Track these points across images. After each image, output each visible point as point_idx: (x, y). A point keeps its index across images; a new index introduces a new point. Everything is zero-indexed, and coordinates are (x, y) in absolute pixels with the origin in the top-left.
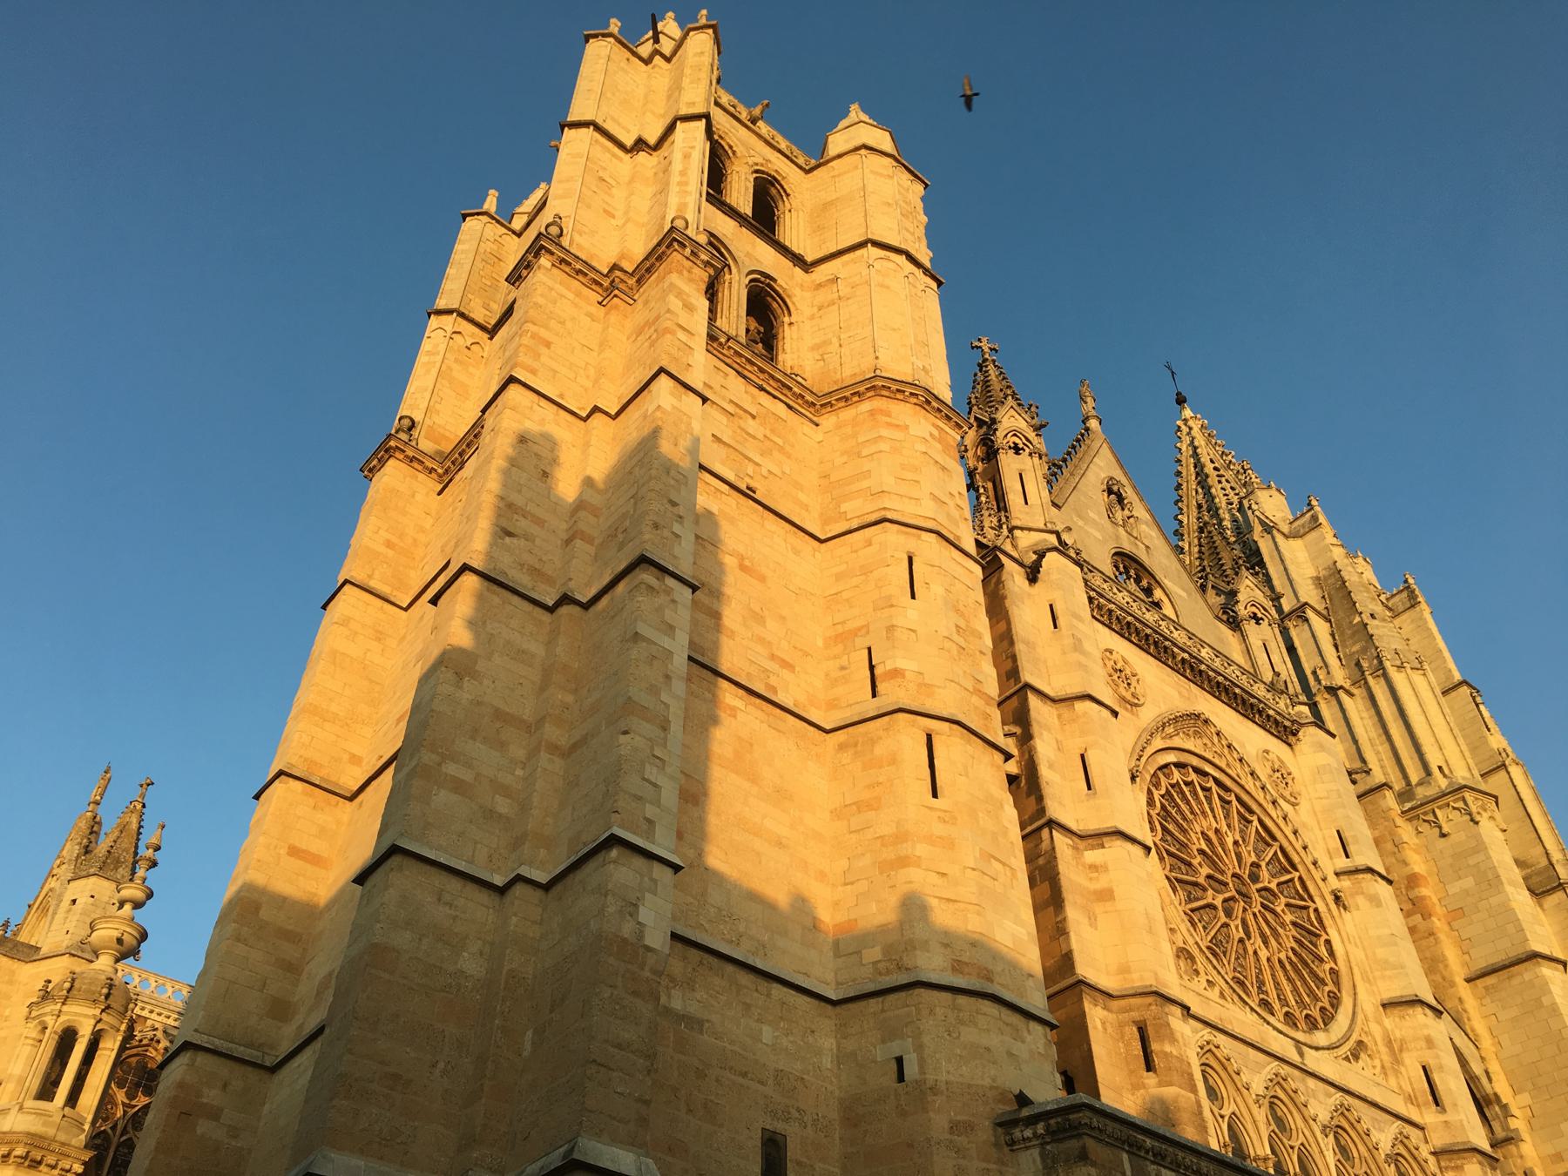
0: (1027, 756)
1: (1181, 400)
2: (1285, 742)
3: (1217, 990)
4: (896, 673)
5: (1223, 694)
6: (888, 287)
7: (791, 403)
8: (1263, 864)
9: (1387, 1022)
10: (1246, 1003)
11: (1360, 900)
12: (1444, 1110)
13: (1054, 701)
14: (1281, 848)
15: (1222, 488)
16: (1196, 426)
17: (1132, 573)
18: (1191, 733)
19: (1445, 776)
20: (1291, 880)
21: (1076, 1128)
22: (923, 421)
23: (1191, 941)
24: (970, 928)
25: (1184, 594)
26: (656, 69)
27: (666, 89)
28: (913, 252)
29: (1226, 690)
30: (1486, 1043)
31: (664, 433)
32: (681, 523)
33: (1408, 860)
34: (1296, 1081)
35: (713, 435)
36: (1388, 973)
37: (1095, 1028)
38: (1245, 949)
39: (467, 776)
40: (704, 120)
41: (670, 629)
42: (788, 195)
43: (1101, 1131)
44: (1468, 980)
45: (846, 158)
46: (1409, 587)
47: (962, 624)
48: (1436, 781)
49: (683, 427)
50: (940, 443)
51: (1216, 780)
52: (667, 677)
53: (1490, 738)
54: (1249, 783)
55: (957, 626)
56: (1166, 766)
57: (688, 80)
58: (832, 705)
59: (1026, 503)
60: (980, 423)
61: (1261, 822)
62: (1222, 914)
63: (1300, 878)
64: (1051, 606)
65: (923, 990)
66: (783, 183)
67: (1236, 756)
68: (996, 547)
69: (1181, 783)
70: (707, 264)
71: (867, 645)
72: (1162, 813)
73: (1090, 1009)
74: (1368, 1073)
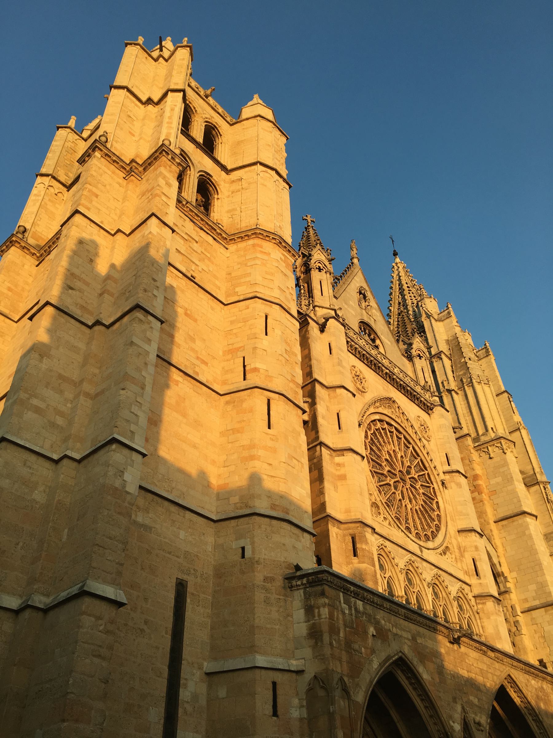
0: (313, 413)
1: (395, 254)
2: (427, 413)
3: (388, 522)
4: (256, 370)
5: (402, 389)
6: (266, 186)
7: (215, 237)
8: (413, 467)
10: (400, 528)
11: (453, 485)
12: (480, 578)
13: (327, 388)
14: (421, 460)
15: (410, 296)
16: (401, 266)
17: (367, 331)
18: (387, 406)
19: (494, 432)
20: (424, 474)
21: (321, 581)
22: (277, 252)
23: (378, 499)
24: (281, 489)
25: (389, 343)
26: (160, 64)
27: (164, 75)
28: (279, 170)
30: (500, 549)
31: (152, 245)
32: (158, 290)
33: (475, 468)
34: (418, 563)
35: (176, 249)
36: (461, 517)
37: (333, 536)
38: (401, 504)
39: (42, 405)
40: (182, 93)
41: (149, 341)
42: (221, 135)
43: (331, 582)
44: (495, 522)
45: (250, 121)
46: (486, 347)
47: (288, 349)
48: (490, 434)
49: (162, 243)
50: (284, 263)
52: (146, 364)
53: (514, 417)
54: (410, 430)
55: (286, 350)
57: (175, 72)
58: (224, 383)
59: (322, 295)
60: (304, 255)
61: (413, 448)
62: (393, 488)
63: (428, 474)
64: (329, 344)
65: (256, 517)
66: (219, 129)
67: (405, 418)
68: (306, 314)
69: (381, 429)
70: (179, 164)
71: (243, 355)
72: (371, 442)
73: (331, 528)
74: (449, 560)
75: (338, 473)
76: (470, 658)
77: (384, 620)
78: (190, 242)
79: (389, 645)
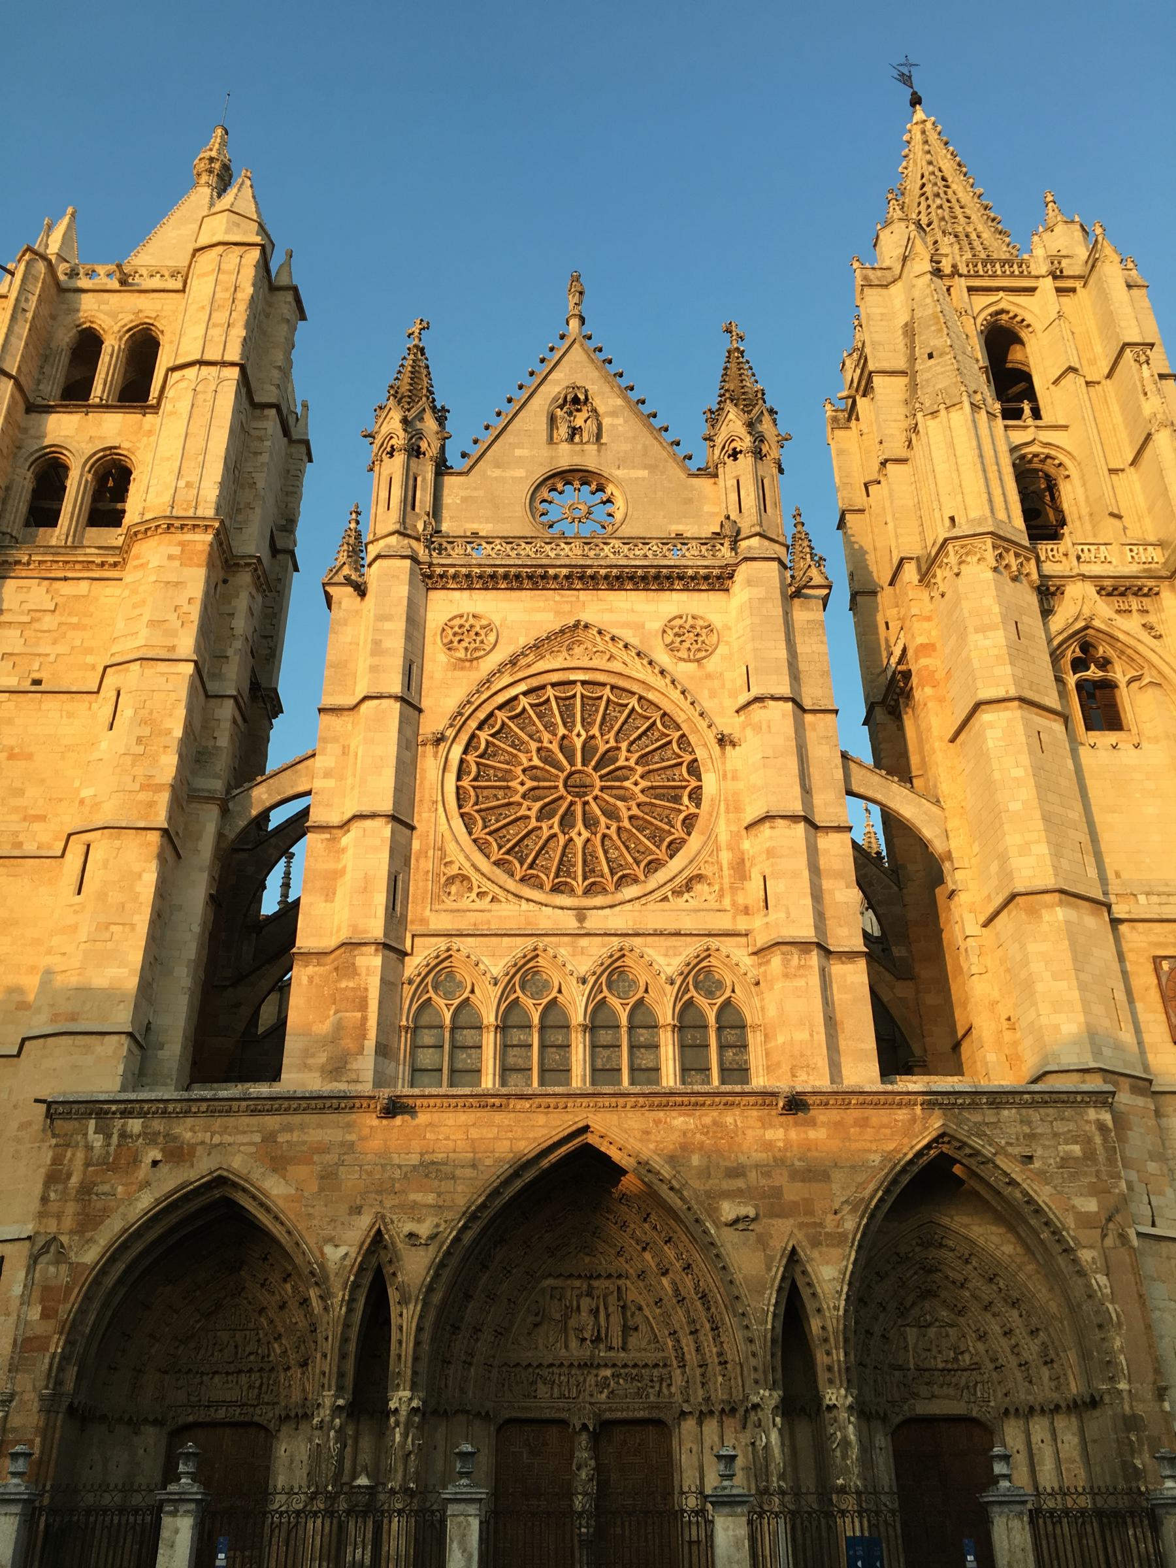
3: (490, 897)
10: (521, 897)
11: (749, 732)
14: (665, 714)
17: (577, 484)
20: (670, 742)
25: (644, 473)
29: (631, 578)
36: (754, 796)
37: (300, 984)
42: (162, 332)
44: (952, 740)
47: (146, 731)
50: (180, 559)
51: (584, 683)
56: (516, 698)
62: (533, 820)
63: (683, 735)
69: (528, 707)
75: (340, 866)
76: (442, 1129)
77: (191, 1130)
78: (38, 620)
79: (192, 1166)
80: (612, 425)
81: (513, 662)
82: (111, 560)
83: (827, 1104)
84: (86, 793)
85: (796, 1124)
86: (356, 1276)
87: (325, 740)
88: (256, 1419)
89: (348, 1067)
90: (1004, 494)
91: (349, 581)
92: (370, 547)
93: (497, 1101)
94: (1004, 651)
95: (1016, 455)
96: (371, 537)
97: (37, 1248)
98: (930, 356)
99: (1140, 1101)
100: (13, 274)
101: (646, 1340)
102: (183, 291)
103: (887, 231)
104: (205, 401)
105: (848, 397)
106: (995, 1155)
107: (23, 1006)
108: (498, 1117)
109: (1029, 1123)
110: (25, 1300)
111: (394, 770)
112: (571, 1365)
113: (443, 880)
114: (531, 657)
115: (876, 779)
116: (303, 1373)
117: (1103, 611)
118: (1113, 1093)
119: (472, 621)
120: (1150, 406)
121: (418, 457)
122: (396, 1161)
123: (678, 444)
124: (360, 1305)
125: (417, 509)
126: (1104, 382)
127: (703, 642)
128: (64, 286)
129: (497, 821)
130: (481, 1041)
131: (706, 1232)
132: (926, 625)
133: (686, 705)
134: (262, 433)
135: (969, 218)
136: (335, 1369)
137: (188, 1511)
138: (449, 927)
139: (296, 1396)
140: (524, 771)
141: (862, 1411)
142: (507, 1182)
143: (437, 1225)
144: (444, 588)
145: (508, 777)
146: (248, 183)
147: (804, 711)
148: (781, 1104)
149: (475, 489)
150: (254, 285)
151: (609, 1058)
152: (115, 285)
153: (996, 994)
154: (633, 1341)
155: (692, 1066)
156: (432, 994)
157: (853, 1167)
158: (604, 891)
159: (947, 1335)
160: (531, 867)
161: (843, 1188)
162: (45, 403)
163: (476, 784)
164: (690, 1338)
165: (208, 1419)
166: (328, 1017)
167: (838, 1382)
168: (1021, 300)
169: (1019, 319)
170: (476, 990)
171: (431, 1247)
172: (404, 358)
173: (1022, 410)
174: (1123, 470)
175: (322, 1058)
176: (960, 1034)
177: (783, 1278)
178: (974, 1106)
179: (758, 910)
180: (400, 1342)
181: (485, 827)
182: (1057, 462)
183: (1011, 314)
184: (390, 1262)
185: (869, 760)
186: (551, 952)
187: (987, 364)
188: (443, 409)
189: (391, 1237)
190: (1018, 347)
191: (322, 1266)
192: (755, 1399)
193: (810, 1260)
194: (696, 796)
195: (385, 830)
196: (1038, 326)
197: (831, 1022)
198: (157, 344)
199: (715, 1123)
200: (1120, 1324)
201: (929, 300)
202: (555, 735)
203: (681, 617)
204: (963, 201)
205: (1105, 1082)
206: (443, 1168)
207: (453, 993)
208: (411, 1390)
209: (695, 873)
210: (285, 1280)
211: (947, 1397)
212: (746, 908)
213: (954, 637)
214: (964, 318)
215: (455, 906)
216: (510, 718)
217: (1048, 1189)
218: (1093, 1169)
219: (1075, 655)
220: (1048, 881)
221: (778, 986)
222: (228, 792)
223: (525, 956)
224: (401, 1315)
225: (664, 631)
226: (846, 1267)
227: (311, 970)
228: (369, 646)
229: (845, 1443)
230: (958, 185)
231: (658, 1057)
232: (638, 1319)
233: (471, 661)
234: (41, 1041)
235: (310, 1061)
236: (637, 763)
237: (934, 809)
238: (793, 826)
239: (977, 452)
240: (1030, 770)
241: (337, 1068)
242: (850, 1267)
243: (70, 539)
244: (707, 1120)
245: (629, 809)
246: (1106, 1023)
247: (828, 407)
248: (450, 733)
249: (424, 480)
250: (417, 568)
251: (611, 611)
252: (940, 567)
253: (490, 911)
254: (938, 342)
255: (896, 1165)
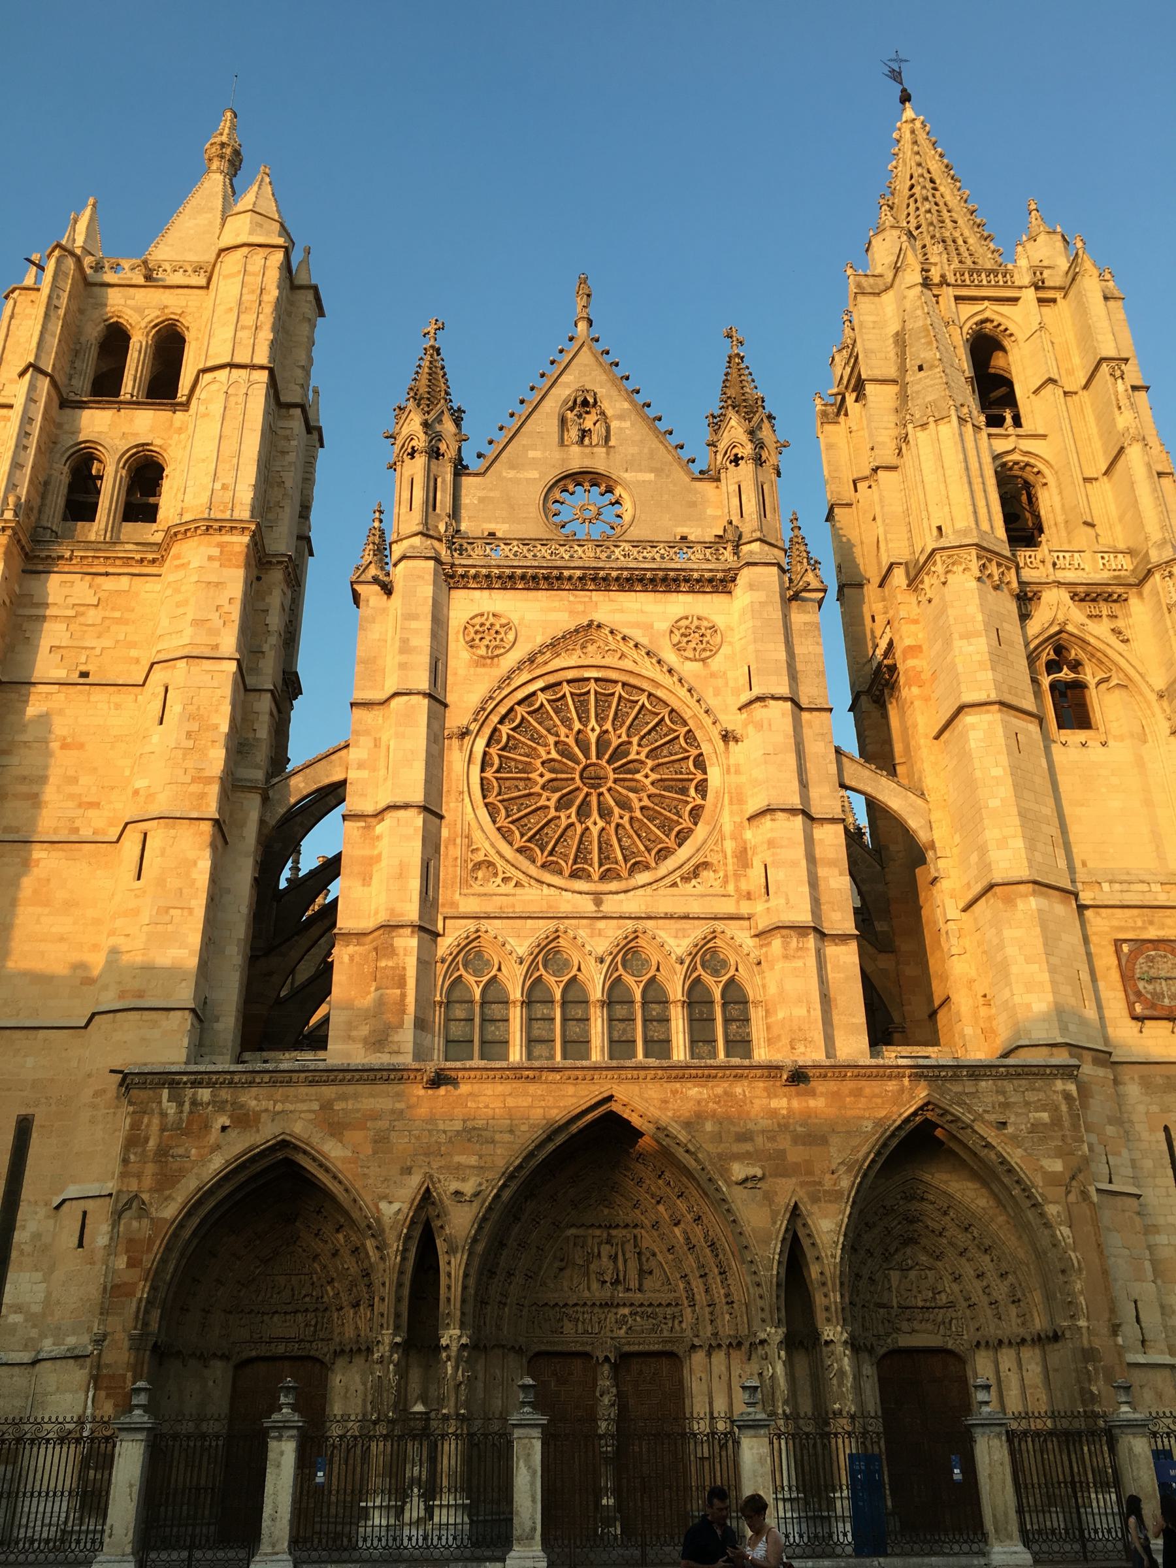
3: (514, 883)
9: (748, 835)
10: (543, 883)
14: (672, 710)
17: (587, 485)
20: (677, 737)
25: (651, 476)
29: (641, 580)
36: (756, 790)
37: (342, 963)
44: (937, 738)
47: (195, 727)
51: (597, 680)
56: (534, 694)
63: (690, 731)
69: (545, 703)
75: (376, 852)
77: (255, 1099)
78: (83, 614)
79: (258, 1131)
80: (621, 429)
81: (532, 660)
82: (150, 557)
83: (825, 1076)
84: (140, 783)
85: (798, 1094)
86: (409, 1229)
87: (357, 733)
88: (312, 1353)
89: (390, 1039)
90: (987, 505)
91: (376, 580)
92: (394, 547)
93: (531, 1074)
94: (986, 657)
95: (998, 462)
96: (394, 537)
97: (120, 1205)
98: (921, 368)
99: (1101, 1072)
100: (42, 269)
101: (659, 1283)
102: (207, 287)
103: (880, 238)
104: (237, 403)
105: (838, 394)
106: (973, 1121)
107: (89, 981)
108: (532, 1088)
109: (1004, 1093)
110: (111, 1250)
111: (424, 763)
112: (594, 1304)
113: (470, 866)
114: (548, 655)
115: (867, 773)
116: (356, 1313)
117: (1076, 617)
118: (1078, 1067)
119: (491, 619)
120: (1124, 420)
121: (437, 459)
122: (441, 1127)
123: (682, 447)
124: (412, 1255)
125: (438, 510)
126: (1080, 392)
127: (708, 642)
128: (91, 280)
129: (519, 810)
130: (508, 1014)
131: (718, 1190)
132: (913, 628)
133: (692, 702)
134: (288, 432)
135: (955, 222)
136: (392, 1310)
137: (292, 1437)
138: (478, 910)
139: (350, 1333)
140: (543, 763)
141: (854, 1345)
142: (540, 1146)
143: (480, 1184)
144: (465, 588)
145: (528, 769)
146: (267, 180)
147: (802, 709)
148: (785, 1077)
149: (491, 490)
150: (278, 287)
151: (624, 1030)
152: (141, 281)
153: (973, 973)
154: (648, 1283)
155: (700, 1037)
156: (462, 971)
157: (848, 1132)
158: (618, 877)
159: (926, 1278)
160: (551, 854)
161: (839, 1151)
162: (78, 398)
163: (499, 775)
164: (700, 1280)
165: (268, 1354)
166: (369, 993)
167: (834, 1320)
168: (1005, 309)
169: (1002, 328)
170: (503, 968)
171: (474, 1204)
172: (421, 359)
173: (1004, 419)
174: (1096, 479)
175: (364, 1031)
176: (937, 1003)
177: (787, 1230)
178: (955, 1078)
179: (760, 896)
180: (449, 1287)
181: (508, 816)
182: (1035, 470)
183: (995, 323)
184: (438, 1216)
185: (856, 754)
186: (571, 933)
187: (972, 374)
188: (459, 410)
189: (438, 1194)
190: (1000, 354)
191: (378, 1220)
192: (763, 1336)
193: (810, 1214)
194: (702, 788)
195: (417, 820)
196: (1020, 335)
197: (826, 999)
198: (185, 341)
199: (726, 1093)
200: (1080, 1269)
201: (919, 312)
202: (571, 729)
203: (687, 618)
204: (950, 204)
205: (1072, 1056)
206: (484, 1133)
207: (481, 971)
208: (460, 1329)
209: (702, 860)
210: (338, 1231)
211: (925, 1331)
212: (749, 893)
213: (940, 642)
214: (951, 328)
215: (482, 890)
216: (528, 713)
217: (1020, 1152)
218: (1060, 1134)
219: (1050, 657)
220: (1024, 873)
221: (778, 966)
222: (267, 781)
223: (547, 937)
224: (449, 1263)
225: (672, 632)
226: (842, 1220)
227: (351, 949)
228: (397, 644)
229: (841, 1373)
230: (946, 188)
231: (669, 1029)
232: (653, 1263)
233: (492, 658)
234: (111, 1015)
235: (354, 1033)
236: (647, 757)
237: (919, 801)
238: (792, 818)
239: (963, 465)
240: (1008, 769)
241: (379, 1040)
242: (846, 1220)
243: (108, 535)
244: (719, 1091)
245: (640, 800)
246: (1072, 1001)
247: (818, 401)
248: (474, 727)
249: (444, 481)
250: (440, 568)
251: (622, 611)
252: (928, 574)
253: (514, 895)
254: (928, 354)
255: (886, 1130)
